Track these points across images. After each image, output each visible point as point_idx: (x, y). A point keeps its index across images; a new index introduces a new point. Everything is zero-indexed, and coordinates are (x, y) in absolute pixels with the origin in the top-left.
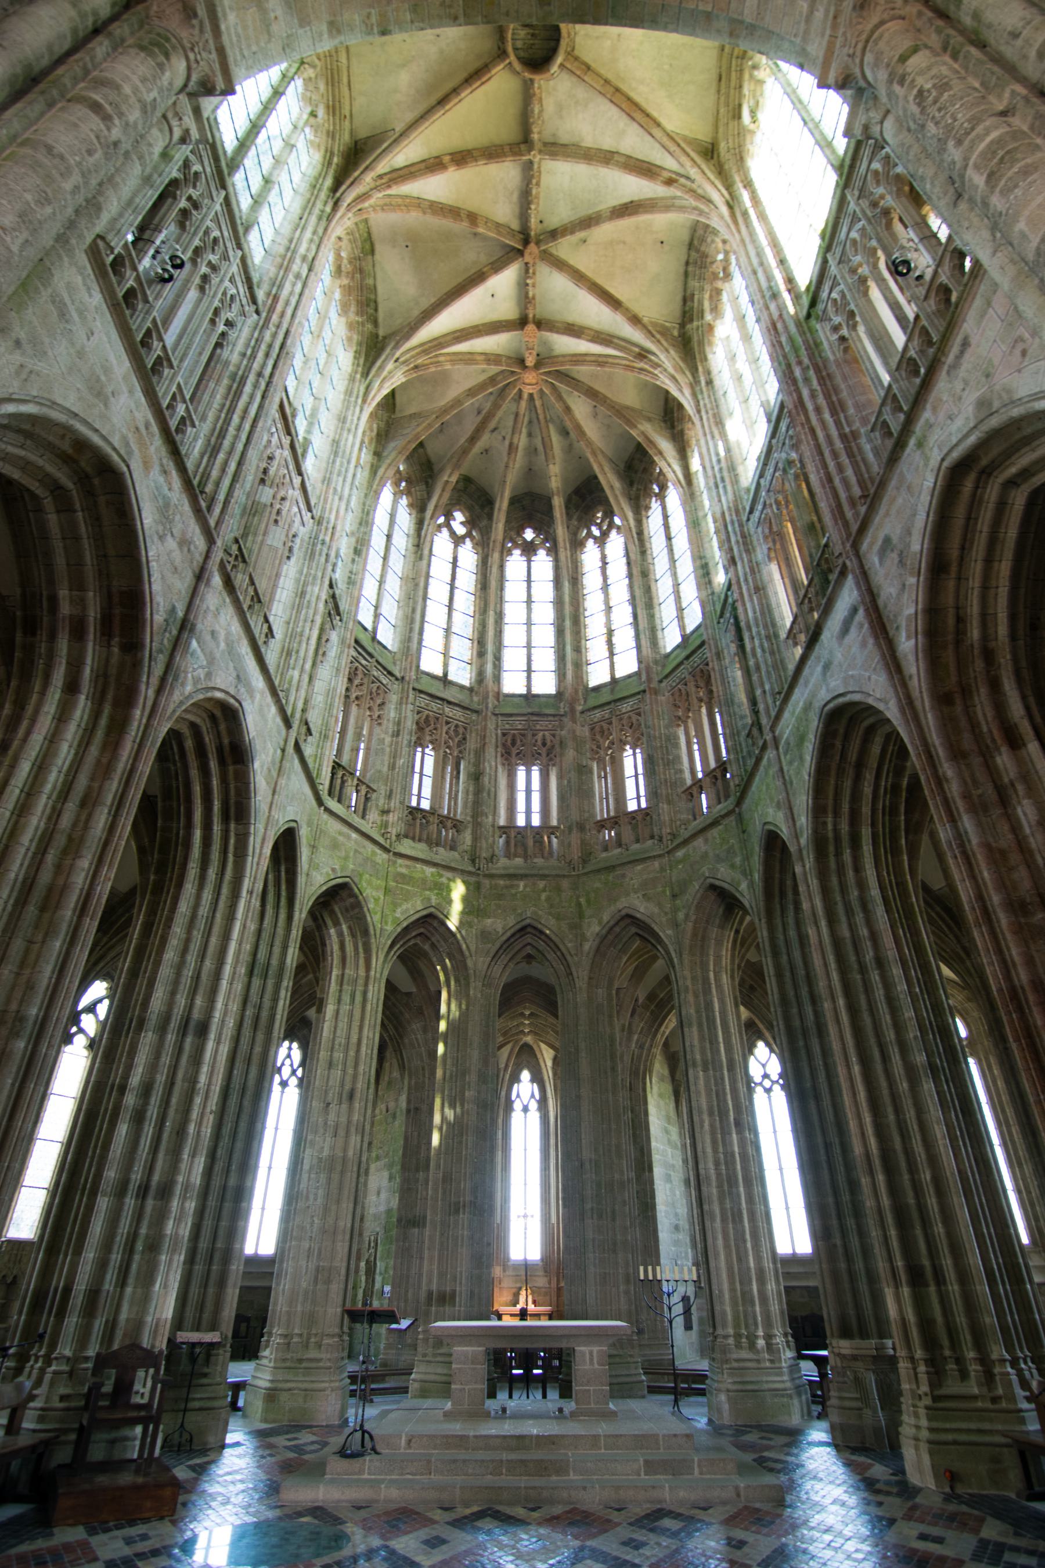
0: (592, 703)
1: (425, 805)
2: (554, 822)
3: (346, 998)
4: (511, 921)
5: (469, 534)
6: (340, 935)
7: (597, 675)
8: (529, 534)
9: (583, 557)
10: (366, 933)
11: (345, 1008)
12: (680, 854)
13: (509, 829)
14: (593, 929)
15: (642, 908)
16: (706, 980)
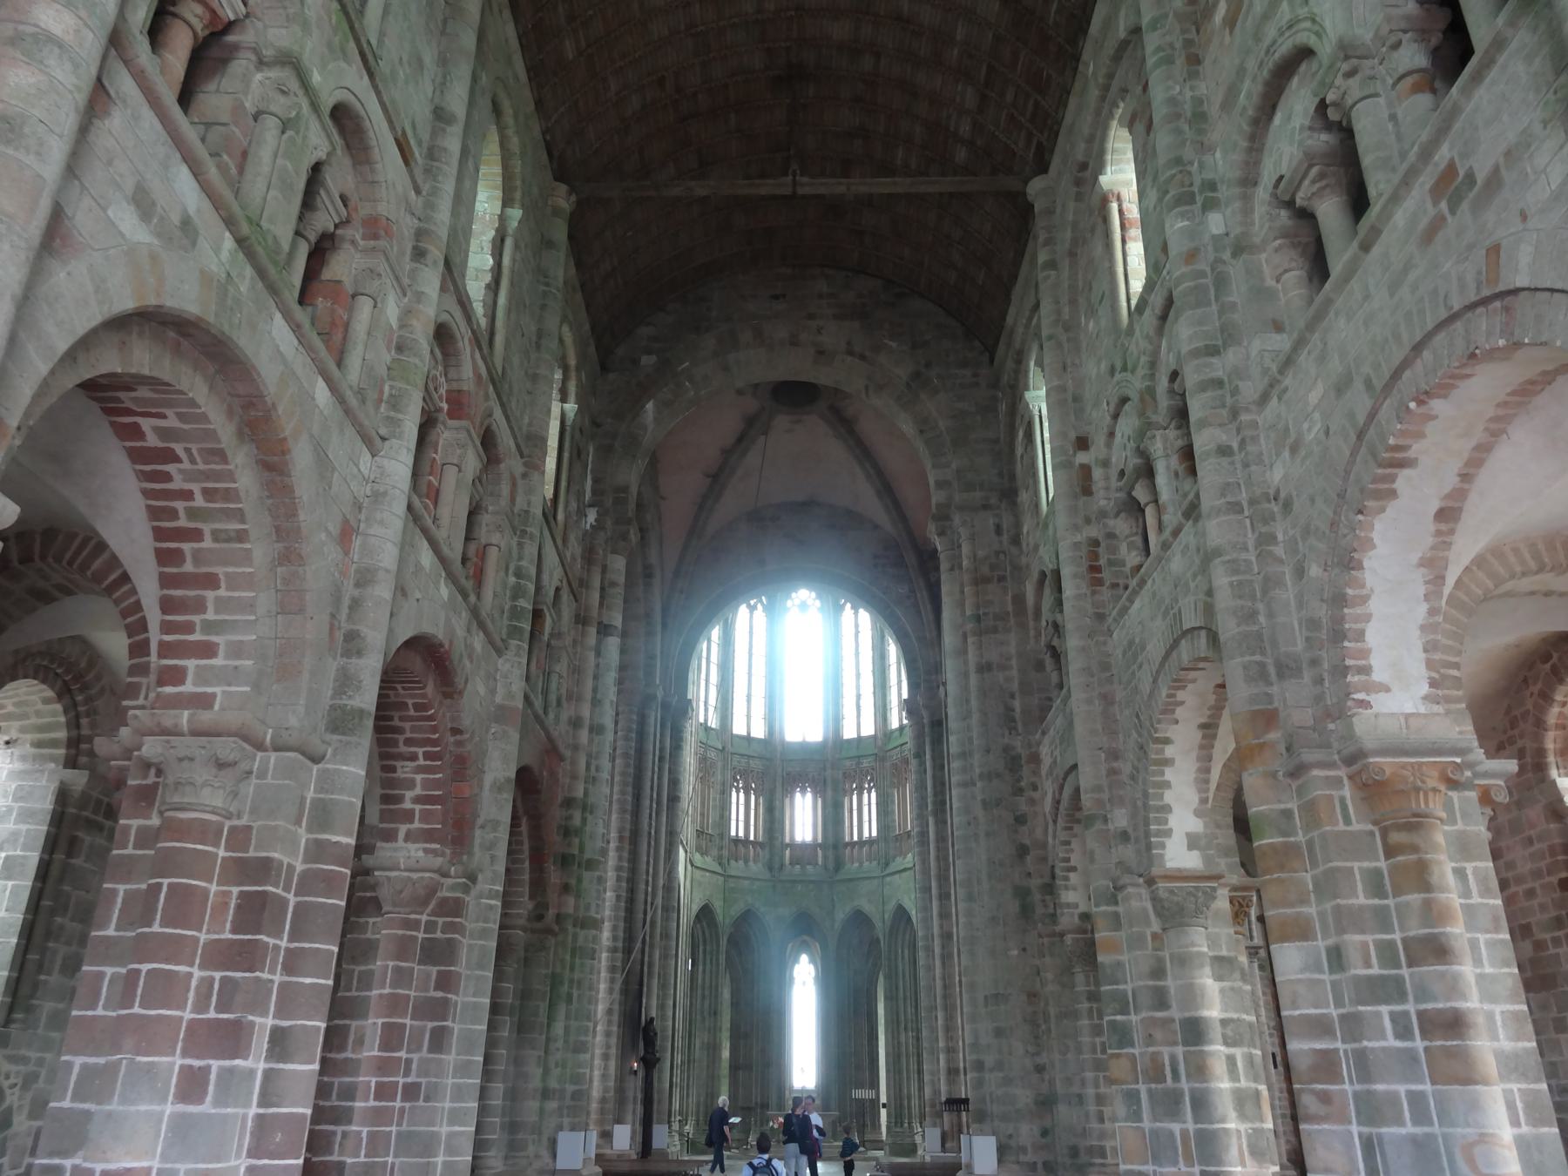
2: (820, 841)
3: (708, 961)
6: (702, 927)
7: (849, 733)
10: (716, 925)
11: (708, 967)
12: (888, 879)
13: (793, 846)
15: (868, 908)
16: (896, 952)
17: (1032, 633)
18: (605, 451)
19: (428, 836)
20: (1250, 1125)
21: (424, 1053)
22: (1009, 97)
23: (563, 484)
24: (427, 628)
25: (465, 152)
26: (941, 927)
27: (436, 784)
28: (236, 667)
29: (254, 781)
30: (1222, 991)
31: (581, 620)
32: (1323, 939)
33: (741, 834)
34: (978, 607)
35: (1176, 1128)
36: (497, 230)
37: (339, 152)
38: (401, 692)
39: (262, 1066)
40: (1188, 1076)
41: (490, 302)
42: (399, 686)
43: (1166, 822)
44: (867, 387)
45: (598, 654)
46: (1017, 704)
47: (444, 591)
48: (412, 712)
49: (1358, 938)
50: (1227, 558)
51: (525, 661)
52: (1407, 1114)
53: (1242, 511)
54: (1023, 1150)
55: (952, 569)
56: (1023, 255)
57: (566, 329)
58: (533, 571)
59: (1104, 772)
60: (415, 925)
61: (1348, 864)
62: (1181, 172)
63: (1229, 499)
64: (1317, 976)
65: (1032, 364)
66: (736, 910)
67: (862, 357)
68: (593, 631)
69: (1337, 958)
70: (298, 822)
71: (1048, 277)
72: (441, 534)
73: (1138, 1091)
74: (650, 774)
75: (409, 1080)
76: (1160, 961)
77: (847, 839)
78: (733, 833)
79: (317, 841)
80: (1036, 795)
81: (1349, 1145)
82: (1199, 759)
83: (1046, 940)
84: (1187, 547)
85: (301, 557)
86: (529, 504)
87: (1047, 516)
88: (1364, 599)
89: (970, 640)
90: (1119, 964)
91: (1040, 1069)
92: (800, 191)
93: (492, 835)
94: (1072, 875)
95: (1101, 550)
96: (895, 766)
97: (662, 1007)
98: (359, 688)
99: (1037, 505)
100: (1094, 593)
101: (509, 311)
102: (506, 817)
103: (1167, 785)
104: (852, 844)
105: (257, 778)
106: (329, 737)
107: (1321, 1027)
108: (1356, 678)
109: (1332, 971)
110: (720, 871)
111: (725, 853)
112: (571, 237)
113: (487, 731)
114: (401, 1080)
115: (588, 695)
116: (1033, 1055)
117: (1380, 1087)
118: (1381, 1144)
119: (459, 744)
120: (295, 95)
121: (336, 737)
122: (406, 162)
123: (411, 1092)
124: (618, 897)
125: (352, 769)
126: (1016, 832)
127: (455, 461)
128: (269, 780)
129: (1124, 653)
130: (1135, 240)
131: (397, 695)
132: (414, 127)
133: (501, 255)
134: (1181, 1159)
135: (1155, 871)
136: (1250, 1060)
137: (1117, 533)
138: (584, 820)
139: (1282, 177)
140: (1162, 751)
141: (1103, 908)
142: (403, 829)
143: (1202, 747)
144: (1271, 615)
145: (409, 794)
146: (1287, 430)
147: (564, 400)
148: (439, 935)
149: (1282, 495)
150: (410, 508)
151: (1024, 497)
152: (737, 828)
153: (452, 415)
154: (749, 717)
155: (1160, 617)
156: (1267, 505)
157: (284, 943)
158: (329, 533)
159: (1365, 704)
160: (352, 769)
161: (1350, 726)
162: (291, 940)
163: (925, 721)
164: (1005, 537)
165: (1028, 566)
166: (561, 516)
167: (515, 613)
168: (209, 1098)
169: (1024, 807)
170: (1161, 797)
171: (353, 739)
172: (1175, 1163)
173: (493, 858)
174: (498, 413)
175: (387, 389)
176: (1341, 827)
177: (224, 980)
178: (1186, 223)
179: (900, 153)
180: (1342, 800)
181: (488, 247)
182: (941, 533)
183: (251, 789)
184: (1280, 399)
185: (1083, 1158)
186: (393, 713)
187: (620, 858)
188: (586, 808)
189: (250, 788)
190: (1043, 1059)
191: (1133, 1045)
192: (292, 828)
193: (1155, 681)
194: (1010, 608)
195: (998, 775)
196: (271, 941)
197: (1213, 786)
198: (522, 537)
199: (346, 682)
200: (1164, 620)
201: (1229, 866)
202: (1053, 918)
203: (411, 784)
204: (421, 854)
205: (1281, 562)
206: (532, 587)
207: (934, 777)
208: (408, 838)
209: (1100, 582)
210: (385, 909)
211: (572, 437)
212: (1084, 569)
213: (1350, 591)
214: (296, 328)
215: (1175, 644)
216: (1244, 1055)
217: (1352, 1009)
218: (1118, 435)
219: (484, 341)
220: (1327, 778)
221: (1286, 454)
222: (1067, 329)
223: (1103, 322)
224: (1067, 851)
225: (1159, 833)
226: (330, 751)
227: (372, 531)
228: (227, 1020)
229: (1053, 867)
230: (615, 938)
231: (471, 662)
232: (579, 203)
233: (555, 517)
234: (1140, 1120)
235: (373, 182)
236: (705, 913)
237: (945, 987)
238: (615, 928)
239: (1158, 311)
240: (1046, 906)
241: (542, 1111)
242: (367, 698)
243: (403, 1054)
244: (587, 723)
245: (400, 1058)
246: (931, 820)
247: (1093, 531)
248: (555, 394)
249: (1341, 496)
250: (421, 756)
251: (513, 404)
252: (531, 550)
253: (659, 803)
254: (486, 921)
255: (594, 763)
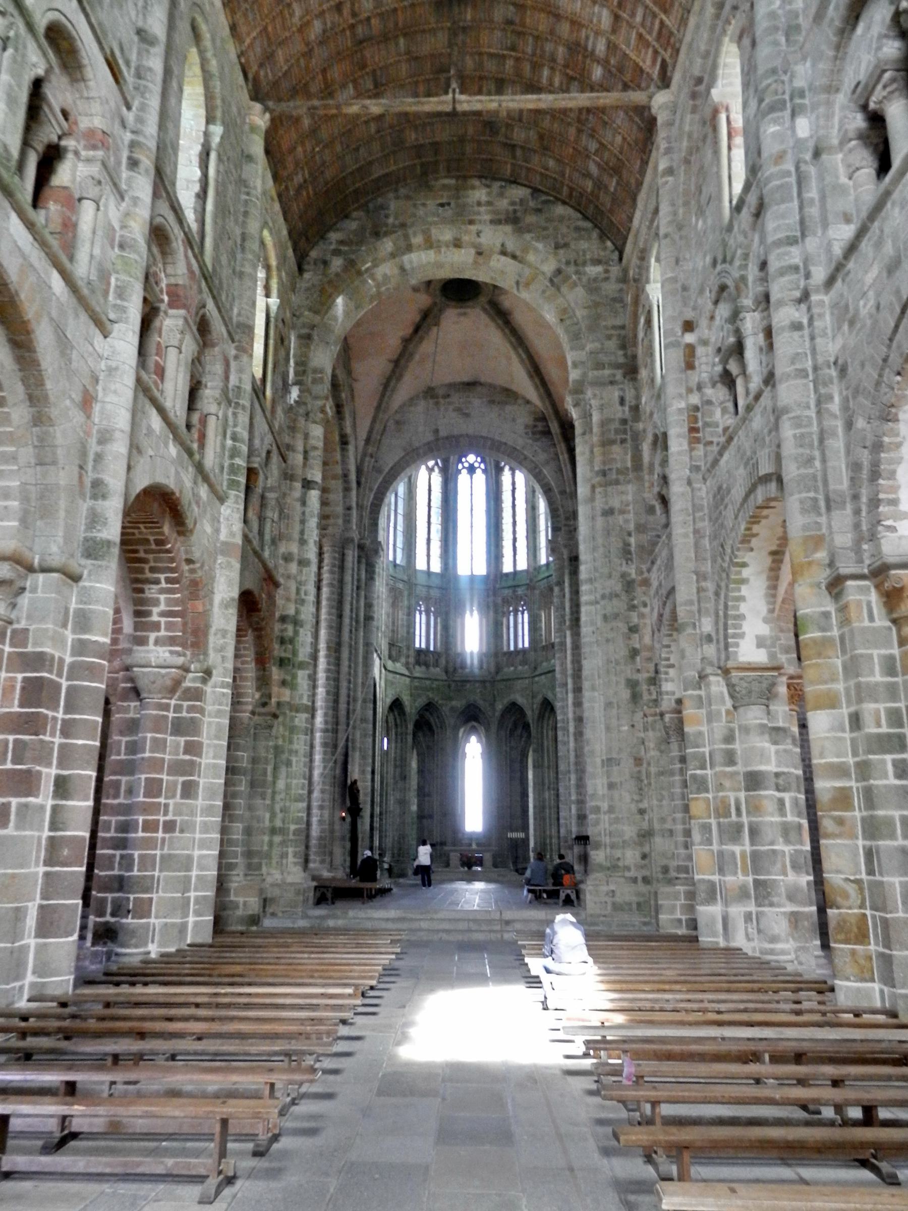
0: (504, 584)
1: (423, 646)
4: (464, 702)
5: (437, 464)
7: (507, 568)
8: (471, 458)
9: (503, 478)
14: (499, 707)
15: (520, 700)
17: (647, 484)
18: (306, 339)
19: (172, 641)
20: (792, 847)
21: (178, 799)
22: (638, 19)
23: (270, 366)
24: (161, 479)
25: (168, 72)
26: (575, 713)
27: (176, 602)
28: (6, 507)
29: (27, 595)
30: (777, 752)
31: (287, 476)
32: (847, 707)
33: (423, 646)
34: (604, 463)
35: (737, 849)
36: (203, 145)
37: (57, 70)
38: (144, 530)
39: (50, 803)
40: (748, 813)
41: (200, 209)
42: (141, 526)
43: (740, 627)
44: (518, 283)
45: (304, 503)
46: (632, 540)
47: (173, 450)
48: (153, 547)
49: (873, 706)
50: (791, 415)
51: (242, 507)
52: (899, 831)
53: (807, 376)
54: (628, 868)
55: (584, 434)
56: (647, 163)
57: (266, 233)
58: (245, 435)
59: (695, 590)
60: (166, 707)
61: (869, 652)
62: (776, 81)
63: (798, 366)
64: (840, 734)
65: (653, 260)
66: (421, 702)
67: (514, 257)
68: (298, 485)
69: (856, 721)
70: (65, 626)
71: (667, 183)
72: (168, 404)
73: (710, 824)
74: (349, 598)
75: (167, 818)
76: (732, 730)
77: (505, 649)
78: (417, 645)
79: (80, 640)
80: (646, 611)
81: (856, 855)
82: (769, 578)
83: (650, 719)
84: (765, 408)
85: (50, 419)
86: (240, 380)
87: (660, 389)
88: (899, 445)
89: (598, 490)
90: (700, 733)
91: (642, 812)
92: (459, 108)
93: (222, 641)
94: (672, 672)
95: (699, 415)
96: (542, 594)
97: (363, 772)
98: (105, 524)
99: (653, 380)
100: (692, 449)
101: (215, 216)
102: (232, 627)
103: (742, 599)
104: (510, 653)
105: (31, 592)
106: (83, 562)
107: (841, 771)
108: (886, 509)
109: (852, 730)
110: (407, 673)
111: (412, 660)
112: (267, 152)
113: (215, 561)
114: (162, 819)
115: (296, 536)
116: (637, 801)
117: (880, 813)
118: (878, 852)
119: (192, 571)
120: (12, 15)
121: (89, 562)
122: (117, 81)
123: (170, 827)
124: (328, 693)
125: (104, 586)
126: (630, 638)
127: (176, 344)
128: (40, 594)
129: (714, 497)
130: (739, 147)
131: (140, 533)
132: (122, 49)
133: (207, 167)
134: (739, 871)
135: (730, 664)
136: (795, 801)
137: (714, 400)
138: (296, 633)
139: (858, 84)
140: (740, 573)
141: (690, 692)
142: (153, 636)
143: (771, 569)
144: (824, 461)
145: (155, 610)
146: (847, 306)
147: (268, 295)
148: (184, 714)
149: (840, 362)
150: (139, 380)
151: (643, 374)
152: (420, 642)
153: (171, 305)
154: (428, 556)
155: (742, 467)
156: (827, 371)
157: (60, 715)
158: (73, 400)
159: (893, 529)
160: (104, 586)
161: (878, 546)
162: (65, 713)
163: (565, 557)
164: (627, 409)
165: (644, 431)
166: (269, 393)
167: (233, 469)
168: (12, 824)
169: (635, 620)
170: (737, 608)
171: (104, 563)
172: (735, 873)
173: (223, 657)
174: (210, 305)
175: (113, 280)
176: (867, 623)
177: (15, 741)
178: (778, 128)
179: (546, 72)
180: (869, 604)
181: (195, 161)
182: (576, 405)
183: (26, 601)
184: (843, 281)
185: (673, 874)
186: (138, 547)
187: (328, 663)
188: (297, 622)
189: (24, 600)
190: (644, 805)
191: (707, 791)
192: (61, 630)
193: (736, 517)
194: (629, 464)
195: (617, 596)
196: (50, 714)
197: (780, 599)
198: (235, 408)
199: (94, 519)
200: (745, 468)
201: (786, 659)
202: (656, 702)
203: (156, 602)
204: (167, 654)
205: (836, 417)
206: (245, 449)
207: (571, 600)
208: (157, 643)
209: (698, 440)
210: (143, 695)
211: (276, 326)
212: (686, 430)
213: (886, 439)
214: (30, 226)
215: (752, 490)
216: (791, 798)
217: (864, 758)
218: (718, 318)
219: (194, 244)
220: (858, 586)
221: (846, 327)
222: (680, 227)
223: (709, 221)
224: (668, 653)
225: (735, 636)
226: (86, 573)
227: (108, 399)
228: (21, 770)
229: (656, 665)
230: (326, 722)
231: (199, 507)
232: (272, 120)
233: (264, 394)
234: (711, 844)
235: (88, 98)
236: (396, 705)
237: (577, 756)
238: (326, 715)
239: (753, 210)
240: (650, 694)
241: (271, 844)
242: (112, 531)
243: (162, 800)
244: (296, 557)
245: (160, 804)
246: (568, 633)
247: (695, 399)
248: (260, 290)
249: (885, 360)
250: (163, 581)
251: (224, 298)
252: (244, 418)
253: (357, 622)
254: (220, 704)
255: (303, 588)
